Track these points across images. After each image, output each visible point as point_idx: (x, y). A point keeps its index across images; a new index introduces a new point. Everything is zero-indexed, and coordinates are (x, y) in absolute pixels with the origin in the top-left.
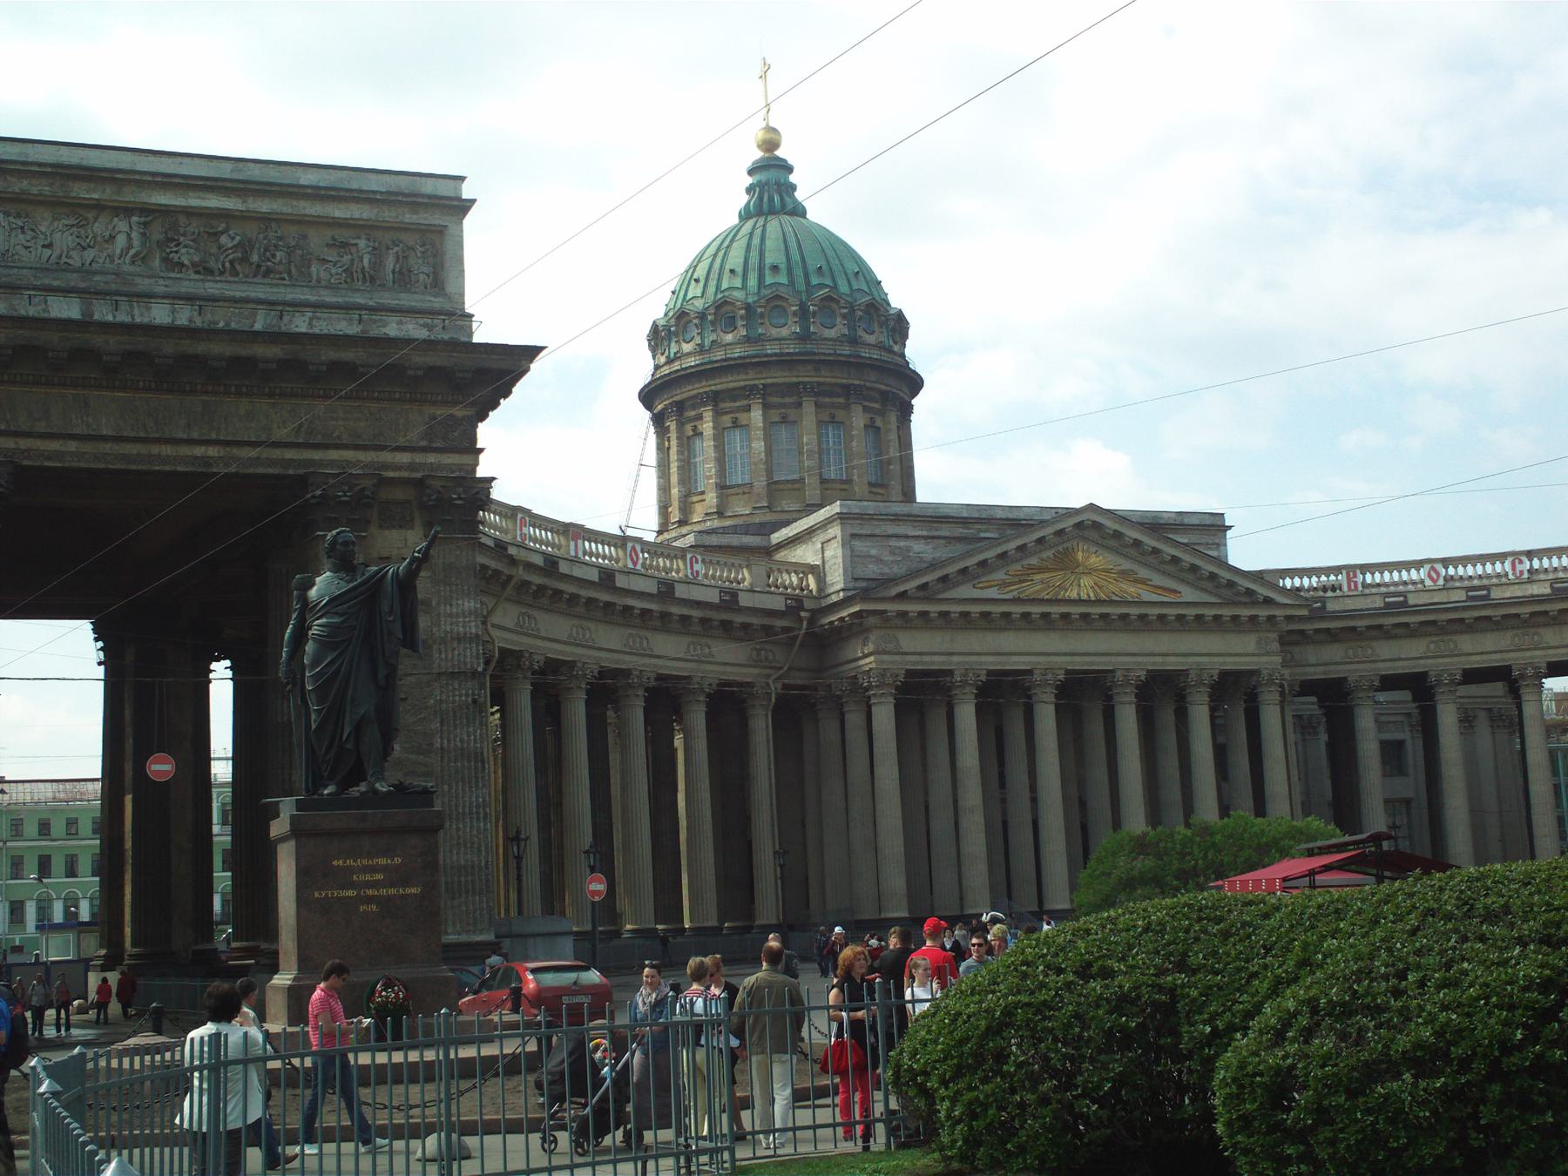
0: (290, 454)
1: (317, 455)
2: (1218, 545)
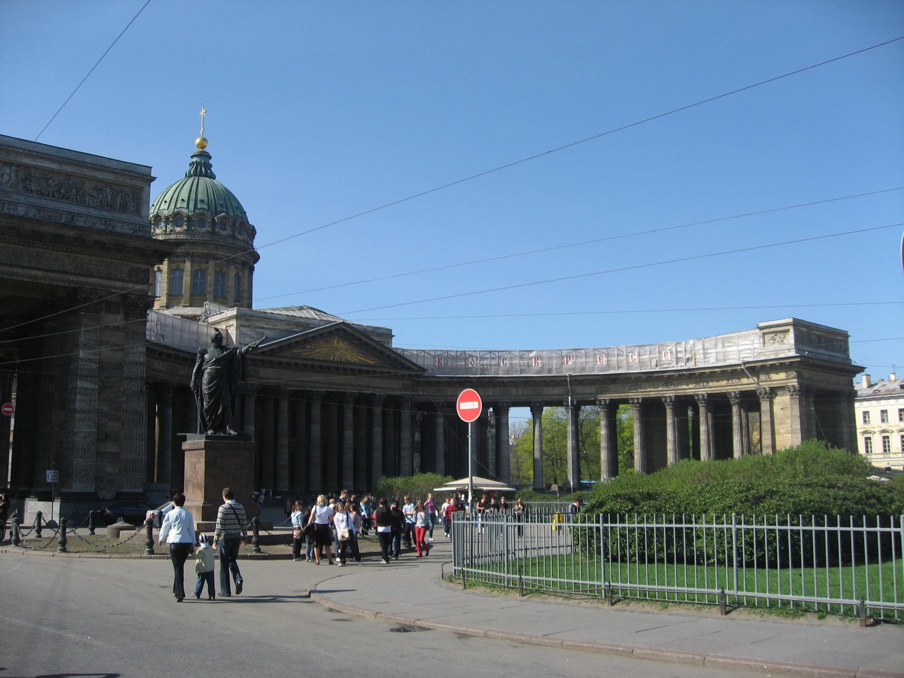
0: (72, 278)
1: (83, 279)
2: (388, 342)
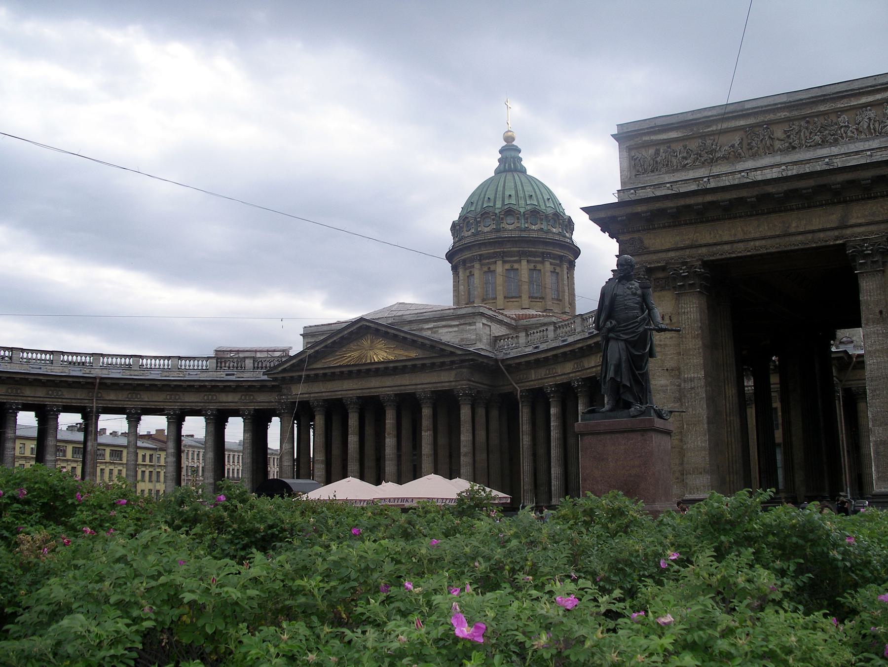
2: (475, 322)
